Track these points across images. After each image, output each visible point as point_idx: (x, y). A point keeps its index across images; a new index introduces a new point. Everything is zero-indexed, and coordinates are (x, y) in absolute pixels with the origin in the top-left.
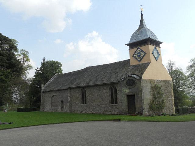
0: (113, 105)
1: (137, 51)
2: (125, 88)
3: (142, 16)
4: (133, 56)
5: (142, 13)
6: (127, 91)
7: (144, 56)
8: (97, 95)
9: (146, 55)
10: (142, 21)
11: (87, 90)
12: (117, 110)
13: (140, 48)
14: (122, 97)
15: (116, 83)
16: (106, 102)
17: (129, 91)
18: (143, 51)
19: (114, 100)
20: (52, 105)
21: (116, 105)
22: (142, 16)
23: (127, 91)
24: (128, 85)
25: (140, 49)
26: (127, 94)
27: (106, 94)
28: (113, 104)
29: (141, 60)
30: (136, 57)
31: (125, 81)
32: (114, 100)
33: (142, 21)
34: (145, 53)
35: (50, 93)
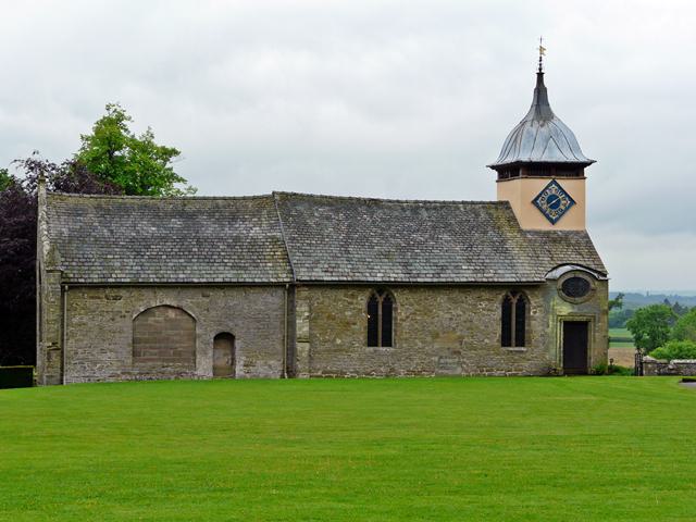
0: (511, 349)
1: (547, 188)
2: (557, 300)
3: (540, 75)
4: (534, 202)
5: (540, 69)
6: (565, 309)
7: (567, 209)
8: (449, 316)
9: (573, 209)
10: (541, 91)
11: (400, 297)
12: (526, 364)
13: (558, 181)
14: (548, 326)
15: (534, 286)
16: (486, 341)
17: (570, 311)
18: (566, 194)
19: (514, 331)
20: (135, 354)
21: (523, 349)
22: (540, 75)
23: (565, 309)
24: (569, 294)
25: (558, 185)
26: (570, 319)
27: (490, 312)
28: (510, 345)
29: (557, 219)
30: (544, 207)
31: (562, 280)
32: (514, 331)
33: (541, 91)
34: (573, 202)
35: (123, 292)
